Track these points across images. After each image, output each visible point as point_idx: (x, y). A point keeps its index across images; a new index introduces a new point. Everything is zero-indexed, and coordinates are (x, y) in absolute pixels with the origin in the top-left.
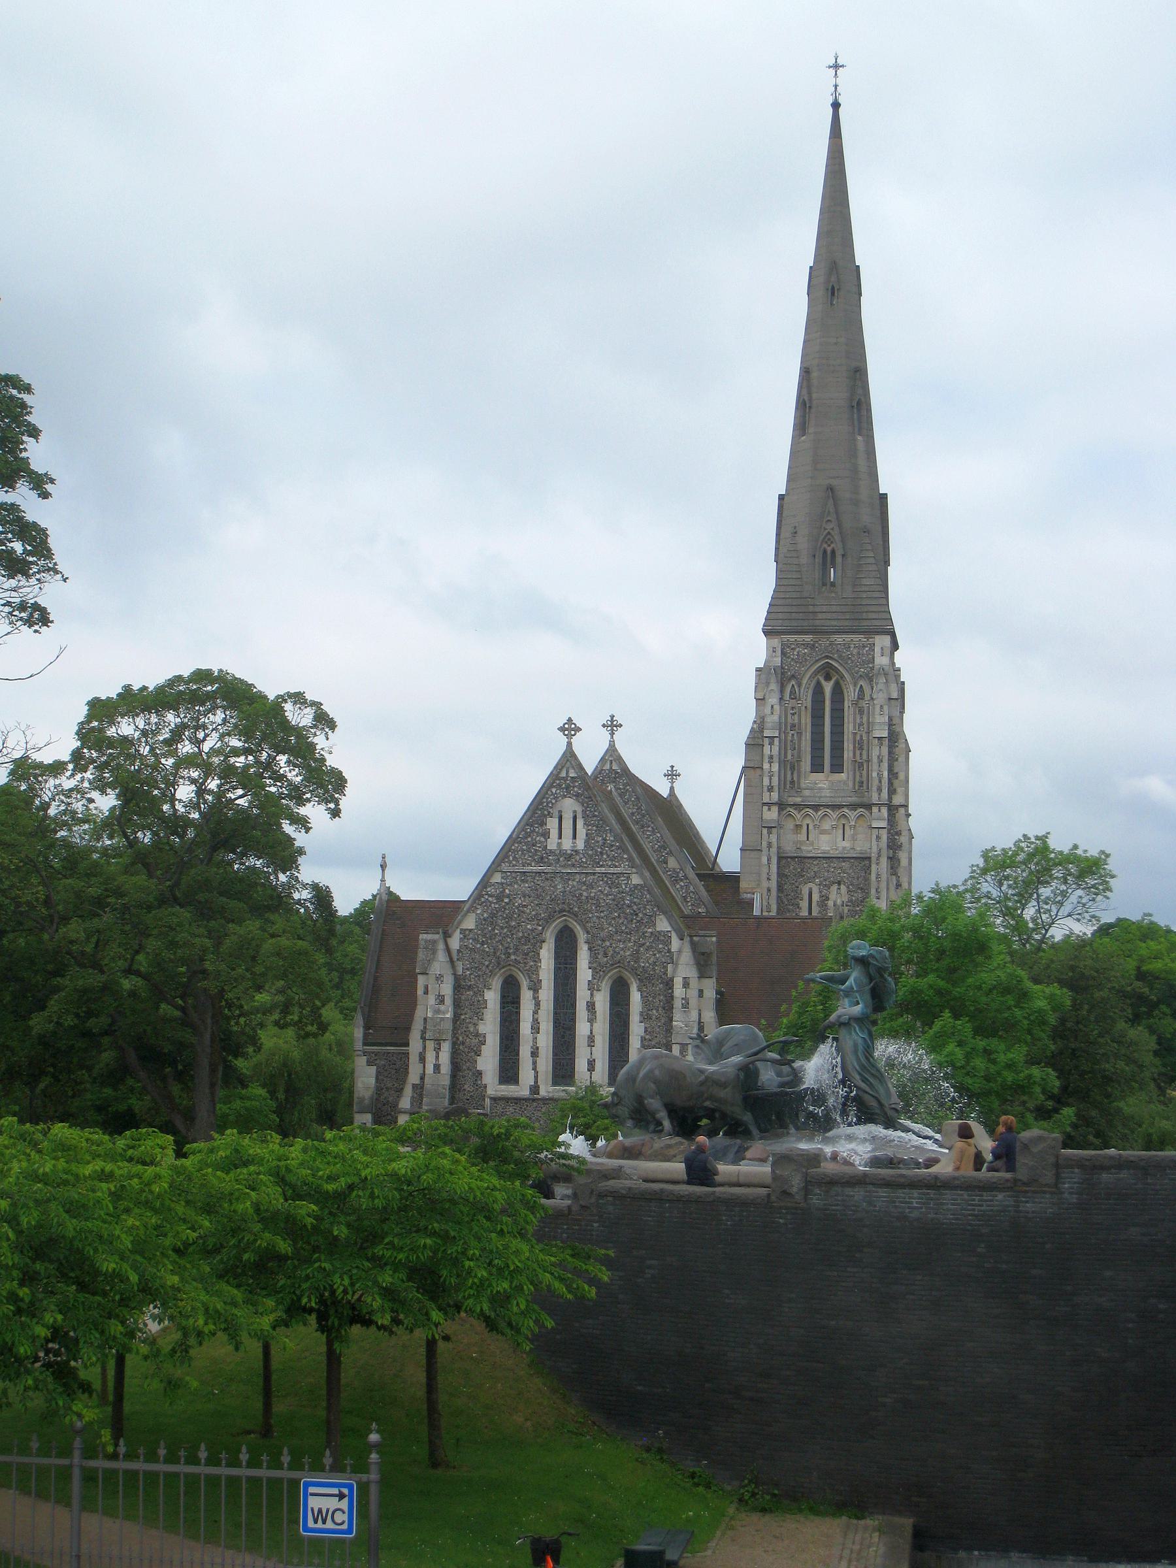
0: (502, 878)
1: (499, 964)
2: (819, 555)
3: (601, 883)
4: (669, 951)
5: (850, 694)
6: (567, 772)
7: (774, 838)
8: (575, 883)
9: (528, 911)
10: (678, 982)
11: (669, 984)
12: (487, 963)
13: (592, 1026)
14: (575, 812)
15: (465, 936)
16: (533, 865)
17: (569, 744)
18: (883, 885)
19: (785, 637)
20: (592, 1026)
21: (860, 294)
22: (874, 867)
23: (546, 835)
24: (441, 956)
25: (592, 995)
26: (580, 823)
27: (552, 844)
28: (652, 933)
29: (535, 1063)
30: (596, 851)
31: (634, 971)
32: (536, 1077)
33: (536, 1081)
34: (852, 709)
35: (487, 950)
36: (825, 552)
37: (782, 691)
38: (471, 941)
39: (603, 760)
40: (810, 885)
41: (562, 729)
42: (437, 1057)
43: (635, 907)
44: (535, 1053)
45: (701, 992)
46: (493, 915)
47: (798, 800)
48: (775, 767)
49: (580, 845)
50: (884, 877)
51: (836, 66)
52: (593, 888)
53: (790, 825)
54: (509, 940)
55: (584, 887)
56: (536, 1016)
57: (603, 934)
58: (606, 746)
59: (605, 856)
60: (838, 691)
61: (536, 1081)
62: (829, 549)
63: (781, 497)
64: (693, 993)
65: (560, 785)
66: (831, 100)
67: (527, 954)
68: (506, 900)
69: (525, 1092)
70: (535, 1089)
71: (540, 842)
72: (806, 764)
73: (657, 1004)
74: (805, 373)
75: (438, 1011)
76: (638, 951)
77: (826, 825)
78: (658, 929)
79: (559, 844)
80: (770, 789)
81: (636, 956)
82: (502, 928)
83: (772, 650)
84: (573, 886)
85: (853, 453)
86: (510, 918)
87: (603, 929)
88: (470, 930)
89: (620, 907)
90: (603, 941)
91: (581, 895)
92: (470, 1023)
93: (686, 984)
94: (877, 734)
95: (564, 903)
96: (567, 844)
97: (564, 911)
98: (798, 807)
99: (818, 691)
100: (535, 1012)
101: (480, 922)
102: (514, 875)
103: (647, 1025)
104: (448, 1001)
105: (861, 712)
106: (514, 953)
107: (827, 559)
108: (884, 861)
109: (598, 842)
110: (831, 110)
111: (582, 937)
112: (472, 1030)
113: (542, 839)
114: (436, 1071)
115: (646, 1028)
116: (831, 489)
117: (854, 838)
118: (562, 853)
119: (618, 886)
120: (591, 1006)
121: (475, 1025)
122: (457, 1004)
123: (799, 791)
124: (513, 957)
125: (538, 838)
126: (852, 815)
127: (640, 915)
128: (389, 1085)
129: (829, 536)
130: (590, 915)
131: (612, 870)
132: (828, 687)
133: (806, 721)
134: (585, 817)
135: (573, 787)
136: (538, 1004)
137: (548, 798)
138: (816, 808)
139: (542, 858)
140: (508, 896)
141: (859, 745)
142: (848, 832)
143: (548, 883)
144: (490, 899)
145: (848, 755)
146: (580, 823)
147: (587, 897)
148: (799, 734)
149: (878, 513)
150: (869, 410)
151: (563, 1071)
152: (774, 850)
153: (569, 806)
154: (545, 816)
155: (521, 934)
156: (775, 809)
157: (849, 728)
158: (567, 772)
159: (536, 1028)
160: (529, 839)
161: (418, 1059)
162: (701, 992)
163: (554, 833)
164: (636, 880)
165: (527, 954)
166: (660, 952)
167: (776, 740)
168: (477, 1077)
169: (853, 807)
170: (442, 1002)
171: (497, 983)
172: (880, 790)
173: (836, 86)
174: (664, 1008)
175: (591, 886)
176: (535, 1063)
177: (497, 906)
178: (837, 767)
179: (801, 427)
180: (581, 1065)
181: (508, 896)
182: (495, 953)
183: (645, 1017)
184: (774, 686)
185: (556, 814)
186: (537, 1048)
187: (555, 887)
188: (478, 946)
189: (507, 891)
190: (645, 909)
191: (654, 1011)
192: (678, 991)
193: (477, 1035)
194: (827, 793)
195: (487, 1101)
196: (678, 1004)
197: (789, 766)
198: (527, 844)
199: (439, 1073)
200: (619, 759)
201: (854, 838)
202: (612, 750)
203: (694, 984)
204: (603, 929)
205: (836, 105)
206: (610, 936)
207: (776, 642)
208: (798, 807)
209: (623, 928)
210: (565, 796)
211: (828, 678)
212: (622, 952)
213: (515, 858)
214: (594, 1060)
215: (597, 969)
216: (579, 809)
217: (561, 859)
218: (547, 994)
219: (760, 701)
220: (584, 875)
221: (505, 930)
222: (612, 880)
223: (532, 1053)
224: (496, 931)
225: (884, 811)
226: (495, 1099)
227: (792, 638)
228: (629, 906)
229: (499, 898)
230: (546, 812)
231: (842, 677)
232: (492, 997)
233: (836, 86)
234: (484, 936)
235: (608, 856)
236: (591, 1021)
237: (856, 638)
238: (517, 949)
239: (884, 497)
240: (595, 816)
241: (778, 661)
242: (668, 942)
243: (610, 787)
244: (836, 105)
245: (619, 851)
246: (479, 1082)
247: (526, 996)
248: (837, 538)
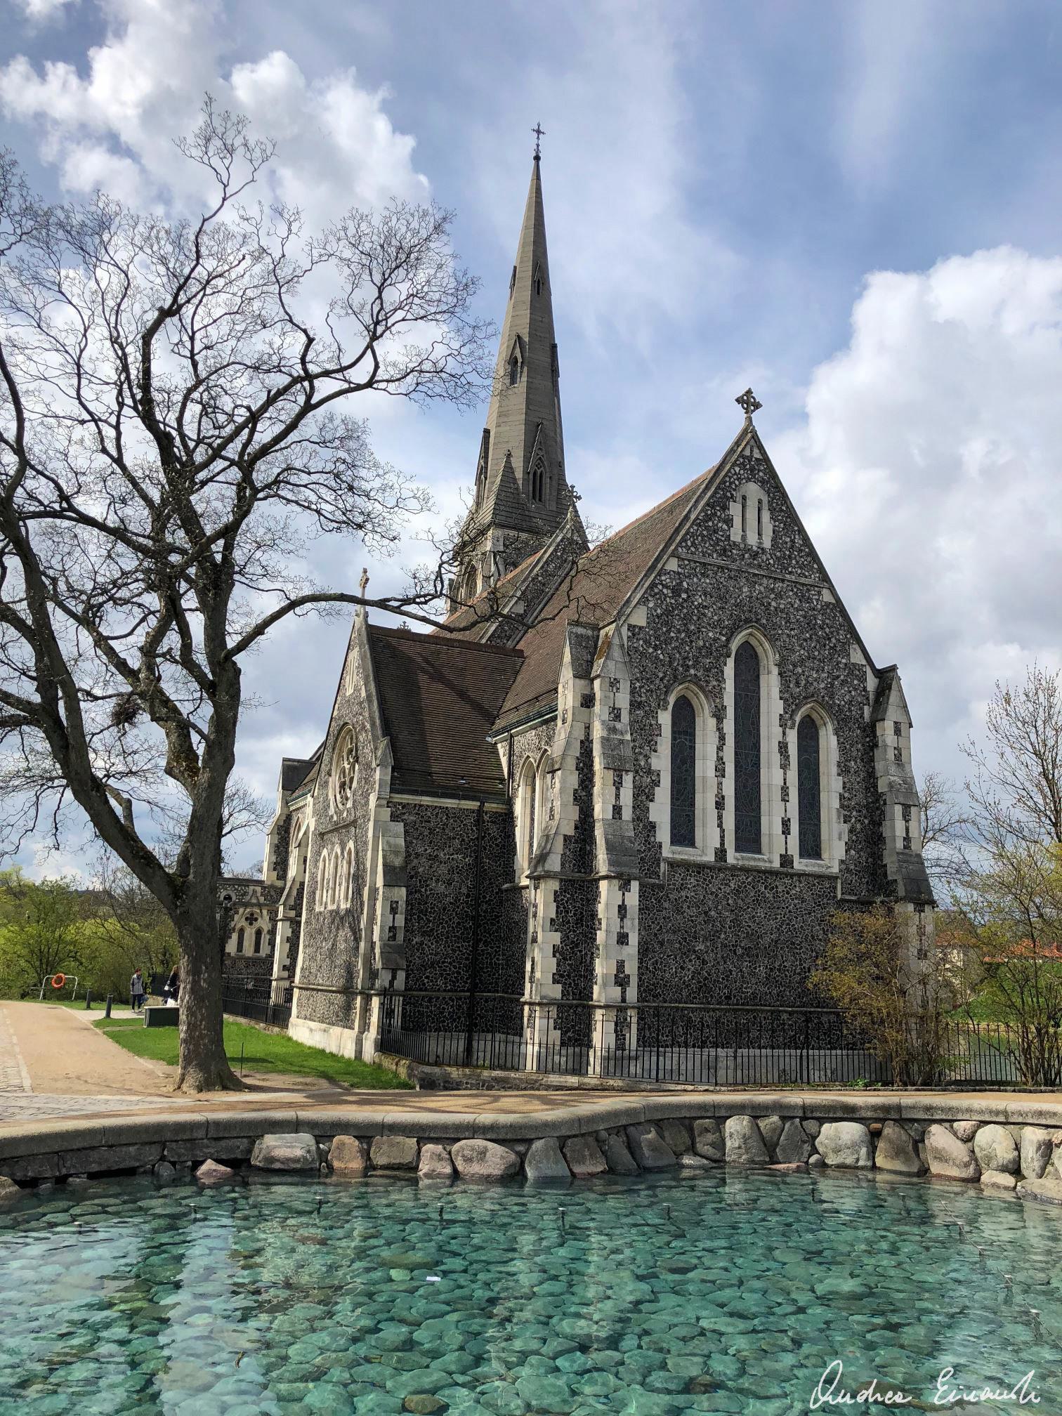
0: (679, 566)
1: (675, 677)
3: (791, 593)
4: (865, 689)
6: (752, 451)
8: (762, 589)
9: (710, 614)
12: (661, 675)
13: (785, 774)
14: (760, 502)
15: (634, 635)
16: (715, 556)
17: (750, 420)
19: (507, 531)
20: (785, 774)
23: (729, 522)
25: (784, 733)
26: (766, 516)
28: (846, 664)
29: (720, 817)
30: (785, 554)
31: (829, 708)
32: (722, 838)
33: (722, 844)
35: (661, 657)
38: (641, 642)
42: (617, 796)
43: (827, 630)
44: (720, 805)
46: (668, 613)
49: (767, 544)
52: (782, 598)
54: (687, 648)
55: (772, 596)
56: (721, 754)
57: (794, 657)
59: (794, 562)
61: (722, 844)
62: (539, 471)
65: (742, 466)
66: (534, 154)
67: (708, 670)
68: (684, 596)
69: (710, 858)
70: (721, 853)
71: (723, 530)
73: (854, 754)
76: (832, 685)
78: (853, 661)
79: (744, 538)
81: (831, 692)
82: (679, 631)
84: (760, 592)
86: (686, 619)
87: (793, 651)
88: (641, 628)
89: (811, 626)
90: (795, 666)
91: (769, 604)
92: (641, 753)
95: (750, 611)
97: (751, 621)
100: (720, 748)
101: (651, 619)
102: (693, 565)
103: (846, 780)
106: (694, 667)
109: (786, 543)
110: (533, 162)
112: (642, 763)
113: (725, 527)
114: (617, 816)
115: (844, 783)
118: (748, 549)
119: (809, 600)
120: (783, 747)
121: (647, 757)
124: (692, 671)
125: (720, 525)
127: (833, 640)
128: (420, 850)
130: (780, 632)
131: (803, 580)
134: (772, 510)
135: (759, 471)
136: (722, 738)
137: (730, 478)
139: (725, 550)
140: (686, 591)
143: (732, 583)
144: (665, 591)
147: (776, 608)
151: (749, 836)
154: (728, 499)
155: (701, 643)
158: (752, 451)
159: (720, 771)
160: (710, 524)
161: (571, 799)
163: (737, 521)
165: (708, 670)
166: (856, 690)
168: (650, 831)
170: (618, 718)
173: (538, 145)
174: (862, 760)
175: (779, 596)
176: (720, 817)
177: (673, 601)
180: (771, 823)
181: (686, 591)
182: (670, 662)
183: (843, 770)
185: (739, 499)
186: (723, 797)
187: (740, 589)
188: (651, 650)
189: (685, 584)
190: (838, 634)
191: (853, 763)
193: (649, 772)
195: (663, 867)
198: (707, 528)
199: (620, 819)
204: (793, 651)
205: (537, 158)
206: (802, 661)
209: (816, 653)
210: (749, 480)
212: (815, 684)
213: (693, 543)
214: (789, 820)
215: (791, 701)
216: (765, 499)
217: (747, 556)
218: (729, 726)
220: (771, 581)
221: (683, 635)
223: (717, 803)
224: (672, 634)
226: (673, 864)
228: (822, 628)
229: (676, 591)
230: (729, 494)
233: (538, 145)
234: (657, 638)
235: (797, 562)
236: (784, 767)
238: (697, 662)
240: (782, 511)
242: (863, 679)
244: (537, 158)
245: (809, 559)
246: (652, 839)
247: (706, 727)
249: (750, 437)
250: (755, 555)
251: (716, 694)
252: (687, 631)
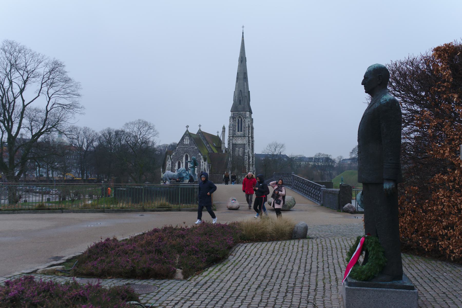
2: (239, 100)
5: (243, 120)
7: (231, 141)
10: (201, 162)
11: (200, 163)
18: (247, 148)
19: (234, 112)
21: (246, 61)
22: (246, 146)
23: (184, 142)
24: (170, 159)
26: (189, 140)
27: (185, 143)
37: (233, 120)
39: (198, 131)
41: (186, 127)
45: (205, 164)
48: (232, 131)
49: (189, 143)
50: (247, 147)
51: (243, 27)
53: (234, 139)
58: (199, 129)
60: (241, 120)
64: (203, 164)
72: (237, 131)
74: (238, 73)
75: (169, 166)
77: (239, 139)
80: (231, 134)
83: (232, 114)
85: (244, 85)
89: (194, 152)
93: (202, 163)
94: (246, 126)
96: (187, 143)
98: (235, 137)
99: (239, 120)
101: (175, 154)
104: (170, 165)
105: (245, 123)
107: (240, 101)
108: (247, 145)
111: (189, 156)
116: (241, 90)
117: (243, 141)
122: (172, 165)
123: (236, 135)
126: (243, 138)
129: (240, 98)
132: (240, 119)
133: (237, 124)
136: (183, 165)
138: (238, 137)
141: (244, 128)
142: (243, 140)
145: (243, 129)
146: (189, 140)
148: (236, 126)
149: (248, 94)
150: (247, 78)
152: (232, 143)
153: (187, 137)
156: (232, 137)
157: (243, 125)
162: (205, 164)
163: (185, 141)
164: (196, 148)
169: (243, 137)
171: (177, 162)
172: (247, 134)
175: (190, 149)
178: (241, 131)
179: (237, 81)
184: (232, 119)
192: (201, 163)
193: (175, 170)
194: (240, 135)
196: (201, 165)
197: (234, 131)
200: (201, 131)
201: (243, 141)
202: (200, 129)
203: (204, 162)
205: (243, 33)
207: (232, 113)
208: (235, 137)
211: (240, 118)
216: (188, 138)
219: (230, 121)
222: (193, 148)
225: (247, 137)
227: (235, 112)
229: (178, 151)
232: (177, 164)
237: (244, 112)
239: (249, 91)
241: (232, 116)
243: (200, 135)
244: (243, 33)
247: (181, 164)
248: (241, 98)
249: (187, 131)
250: (187, 145)
251: (182, 161)
252: (179, 155)
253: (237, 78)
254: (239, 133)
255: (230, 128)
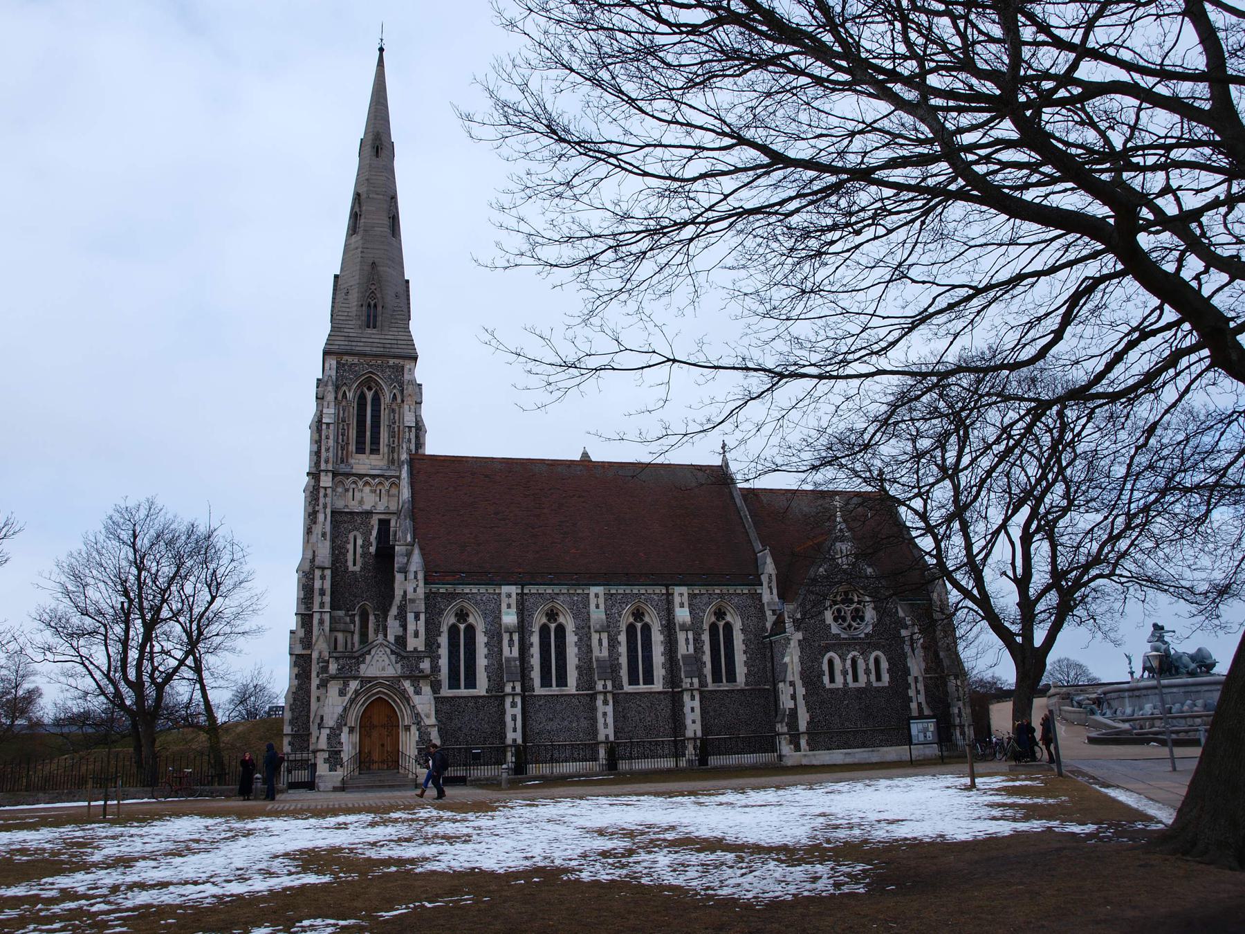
5: (386, 399)
34: (387, 411)
36: (369, 305)
37: (336, 393)
40: (355, 532)
47: (347, 470)
60: (376, 400)
62: (372, 303)
63: (336, 277)
72: (352, 447)
74: (357, 197)
99: (362, 398)
132: (369, 395)
156: (330, 475)
167: (332, 427)
178: (375, 451)
179: (353, 229)
205: (381, 50)
211: (370, 389)
231: (382, 389)
239: (407, 282)
244: (381, 50)
253: (355, 216)
254: (364, 463)
255: (319, 430)
